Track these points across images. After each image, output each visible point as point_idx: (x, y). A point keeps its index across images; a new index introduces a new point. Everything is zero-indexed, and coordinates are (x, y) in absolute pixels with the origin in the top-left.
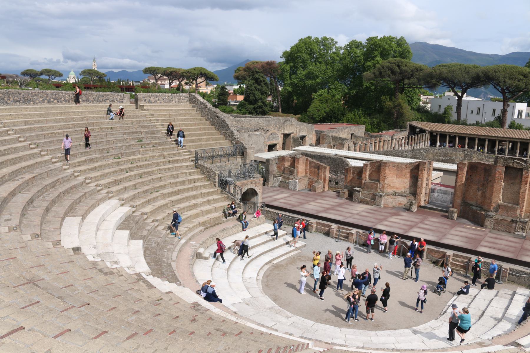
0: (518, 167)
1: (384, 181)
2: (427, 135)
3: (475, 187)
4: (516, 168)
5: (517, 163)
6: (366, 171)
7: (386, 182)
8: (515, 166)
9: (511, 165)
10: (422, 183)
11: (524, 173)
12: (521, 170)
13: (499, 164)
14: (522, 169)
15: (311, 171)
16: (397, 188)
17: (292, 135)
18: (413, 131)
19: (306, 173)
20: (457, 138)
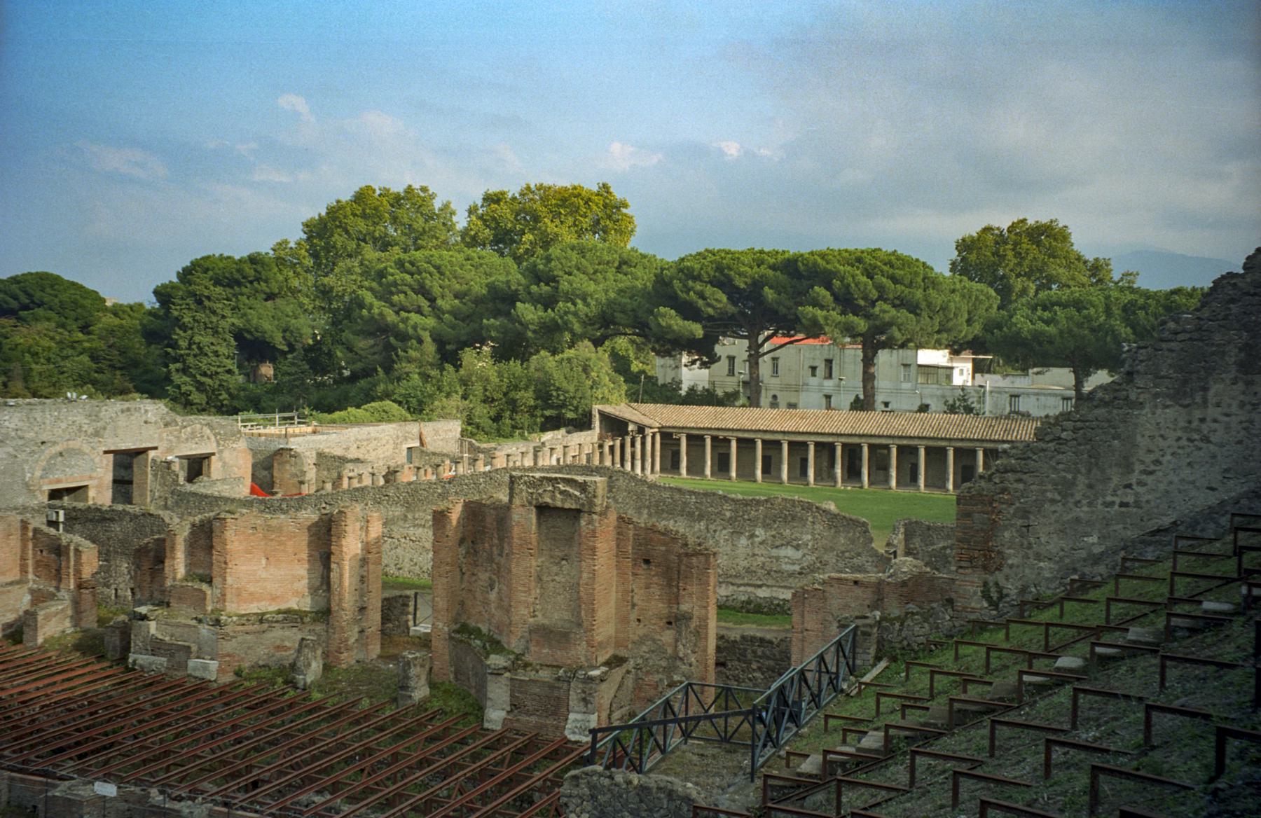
0: (567, 506)
1: (225, 580)
2: (649, 440)
3: (484, 576)
4: (563, 509)
5: (562, 492)
6: (173, 548)
7: (229, 580)
8: (559, 504)
9: (549, 500)
10: (341, 575)
11: (583, 523)
12: (576, 514)
13: (517, 501)
14: (579, 511)
15: (37, 564)
16: (274, 599)
17: (152, 454)
18: (615, 426)
19: (23, 570)
20: (734, 444)
